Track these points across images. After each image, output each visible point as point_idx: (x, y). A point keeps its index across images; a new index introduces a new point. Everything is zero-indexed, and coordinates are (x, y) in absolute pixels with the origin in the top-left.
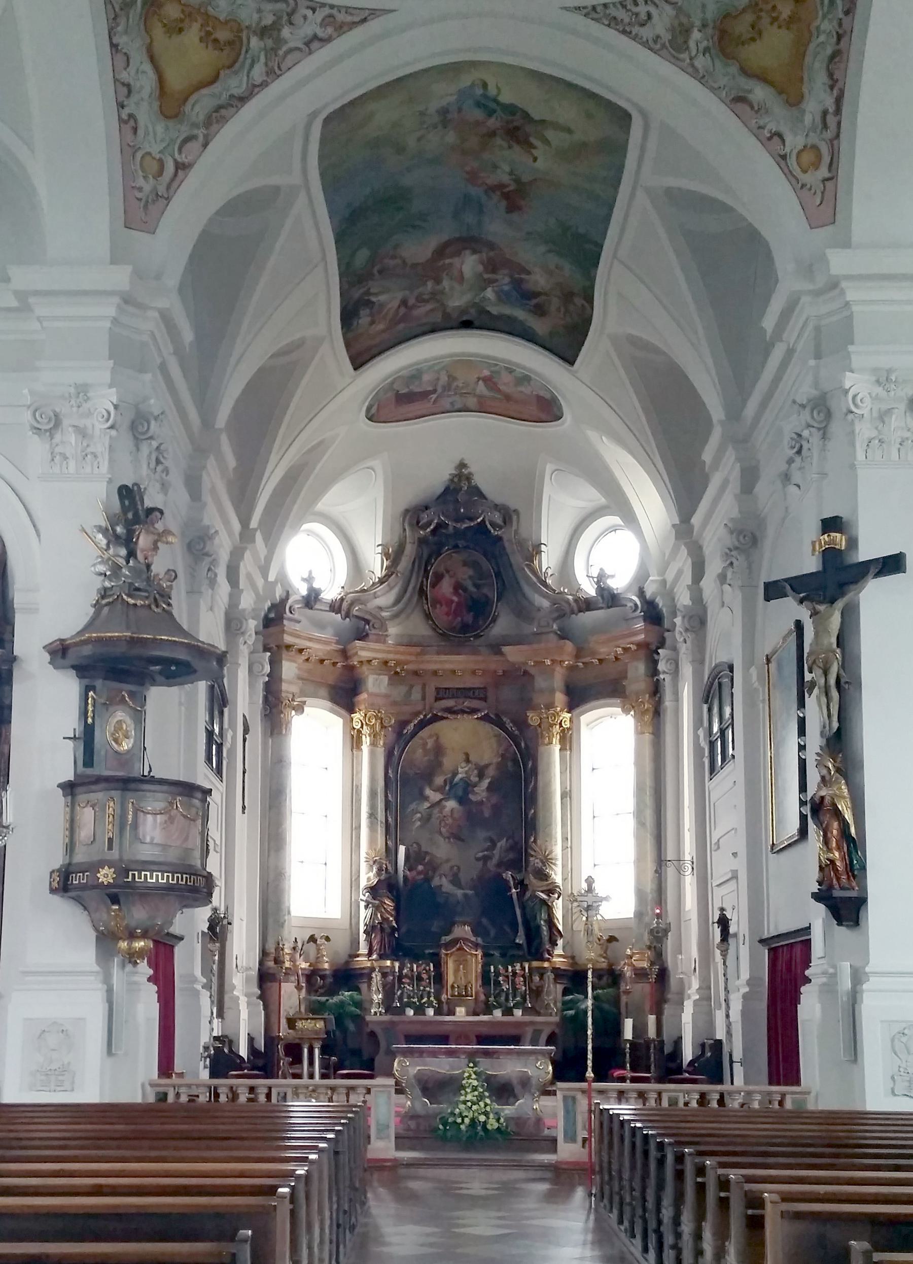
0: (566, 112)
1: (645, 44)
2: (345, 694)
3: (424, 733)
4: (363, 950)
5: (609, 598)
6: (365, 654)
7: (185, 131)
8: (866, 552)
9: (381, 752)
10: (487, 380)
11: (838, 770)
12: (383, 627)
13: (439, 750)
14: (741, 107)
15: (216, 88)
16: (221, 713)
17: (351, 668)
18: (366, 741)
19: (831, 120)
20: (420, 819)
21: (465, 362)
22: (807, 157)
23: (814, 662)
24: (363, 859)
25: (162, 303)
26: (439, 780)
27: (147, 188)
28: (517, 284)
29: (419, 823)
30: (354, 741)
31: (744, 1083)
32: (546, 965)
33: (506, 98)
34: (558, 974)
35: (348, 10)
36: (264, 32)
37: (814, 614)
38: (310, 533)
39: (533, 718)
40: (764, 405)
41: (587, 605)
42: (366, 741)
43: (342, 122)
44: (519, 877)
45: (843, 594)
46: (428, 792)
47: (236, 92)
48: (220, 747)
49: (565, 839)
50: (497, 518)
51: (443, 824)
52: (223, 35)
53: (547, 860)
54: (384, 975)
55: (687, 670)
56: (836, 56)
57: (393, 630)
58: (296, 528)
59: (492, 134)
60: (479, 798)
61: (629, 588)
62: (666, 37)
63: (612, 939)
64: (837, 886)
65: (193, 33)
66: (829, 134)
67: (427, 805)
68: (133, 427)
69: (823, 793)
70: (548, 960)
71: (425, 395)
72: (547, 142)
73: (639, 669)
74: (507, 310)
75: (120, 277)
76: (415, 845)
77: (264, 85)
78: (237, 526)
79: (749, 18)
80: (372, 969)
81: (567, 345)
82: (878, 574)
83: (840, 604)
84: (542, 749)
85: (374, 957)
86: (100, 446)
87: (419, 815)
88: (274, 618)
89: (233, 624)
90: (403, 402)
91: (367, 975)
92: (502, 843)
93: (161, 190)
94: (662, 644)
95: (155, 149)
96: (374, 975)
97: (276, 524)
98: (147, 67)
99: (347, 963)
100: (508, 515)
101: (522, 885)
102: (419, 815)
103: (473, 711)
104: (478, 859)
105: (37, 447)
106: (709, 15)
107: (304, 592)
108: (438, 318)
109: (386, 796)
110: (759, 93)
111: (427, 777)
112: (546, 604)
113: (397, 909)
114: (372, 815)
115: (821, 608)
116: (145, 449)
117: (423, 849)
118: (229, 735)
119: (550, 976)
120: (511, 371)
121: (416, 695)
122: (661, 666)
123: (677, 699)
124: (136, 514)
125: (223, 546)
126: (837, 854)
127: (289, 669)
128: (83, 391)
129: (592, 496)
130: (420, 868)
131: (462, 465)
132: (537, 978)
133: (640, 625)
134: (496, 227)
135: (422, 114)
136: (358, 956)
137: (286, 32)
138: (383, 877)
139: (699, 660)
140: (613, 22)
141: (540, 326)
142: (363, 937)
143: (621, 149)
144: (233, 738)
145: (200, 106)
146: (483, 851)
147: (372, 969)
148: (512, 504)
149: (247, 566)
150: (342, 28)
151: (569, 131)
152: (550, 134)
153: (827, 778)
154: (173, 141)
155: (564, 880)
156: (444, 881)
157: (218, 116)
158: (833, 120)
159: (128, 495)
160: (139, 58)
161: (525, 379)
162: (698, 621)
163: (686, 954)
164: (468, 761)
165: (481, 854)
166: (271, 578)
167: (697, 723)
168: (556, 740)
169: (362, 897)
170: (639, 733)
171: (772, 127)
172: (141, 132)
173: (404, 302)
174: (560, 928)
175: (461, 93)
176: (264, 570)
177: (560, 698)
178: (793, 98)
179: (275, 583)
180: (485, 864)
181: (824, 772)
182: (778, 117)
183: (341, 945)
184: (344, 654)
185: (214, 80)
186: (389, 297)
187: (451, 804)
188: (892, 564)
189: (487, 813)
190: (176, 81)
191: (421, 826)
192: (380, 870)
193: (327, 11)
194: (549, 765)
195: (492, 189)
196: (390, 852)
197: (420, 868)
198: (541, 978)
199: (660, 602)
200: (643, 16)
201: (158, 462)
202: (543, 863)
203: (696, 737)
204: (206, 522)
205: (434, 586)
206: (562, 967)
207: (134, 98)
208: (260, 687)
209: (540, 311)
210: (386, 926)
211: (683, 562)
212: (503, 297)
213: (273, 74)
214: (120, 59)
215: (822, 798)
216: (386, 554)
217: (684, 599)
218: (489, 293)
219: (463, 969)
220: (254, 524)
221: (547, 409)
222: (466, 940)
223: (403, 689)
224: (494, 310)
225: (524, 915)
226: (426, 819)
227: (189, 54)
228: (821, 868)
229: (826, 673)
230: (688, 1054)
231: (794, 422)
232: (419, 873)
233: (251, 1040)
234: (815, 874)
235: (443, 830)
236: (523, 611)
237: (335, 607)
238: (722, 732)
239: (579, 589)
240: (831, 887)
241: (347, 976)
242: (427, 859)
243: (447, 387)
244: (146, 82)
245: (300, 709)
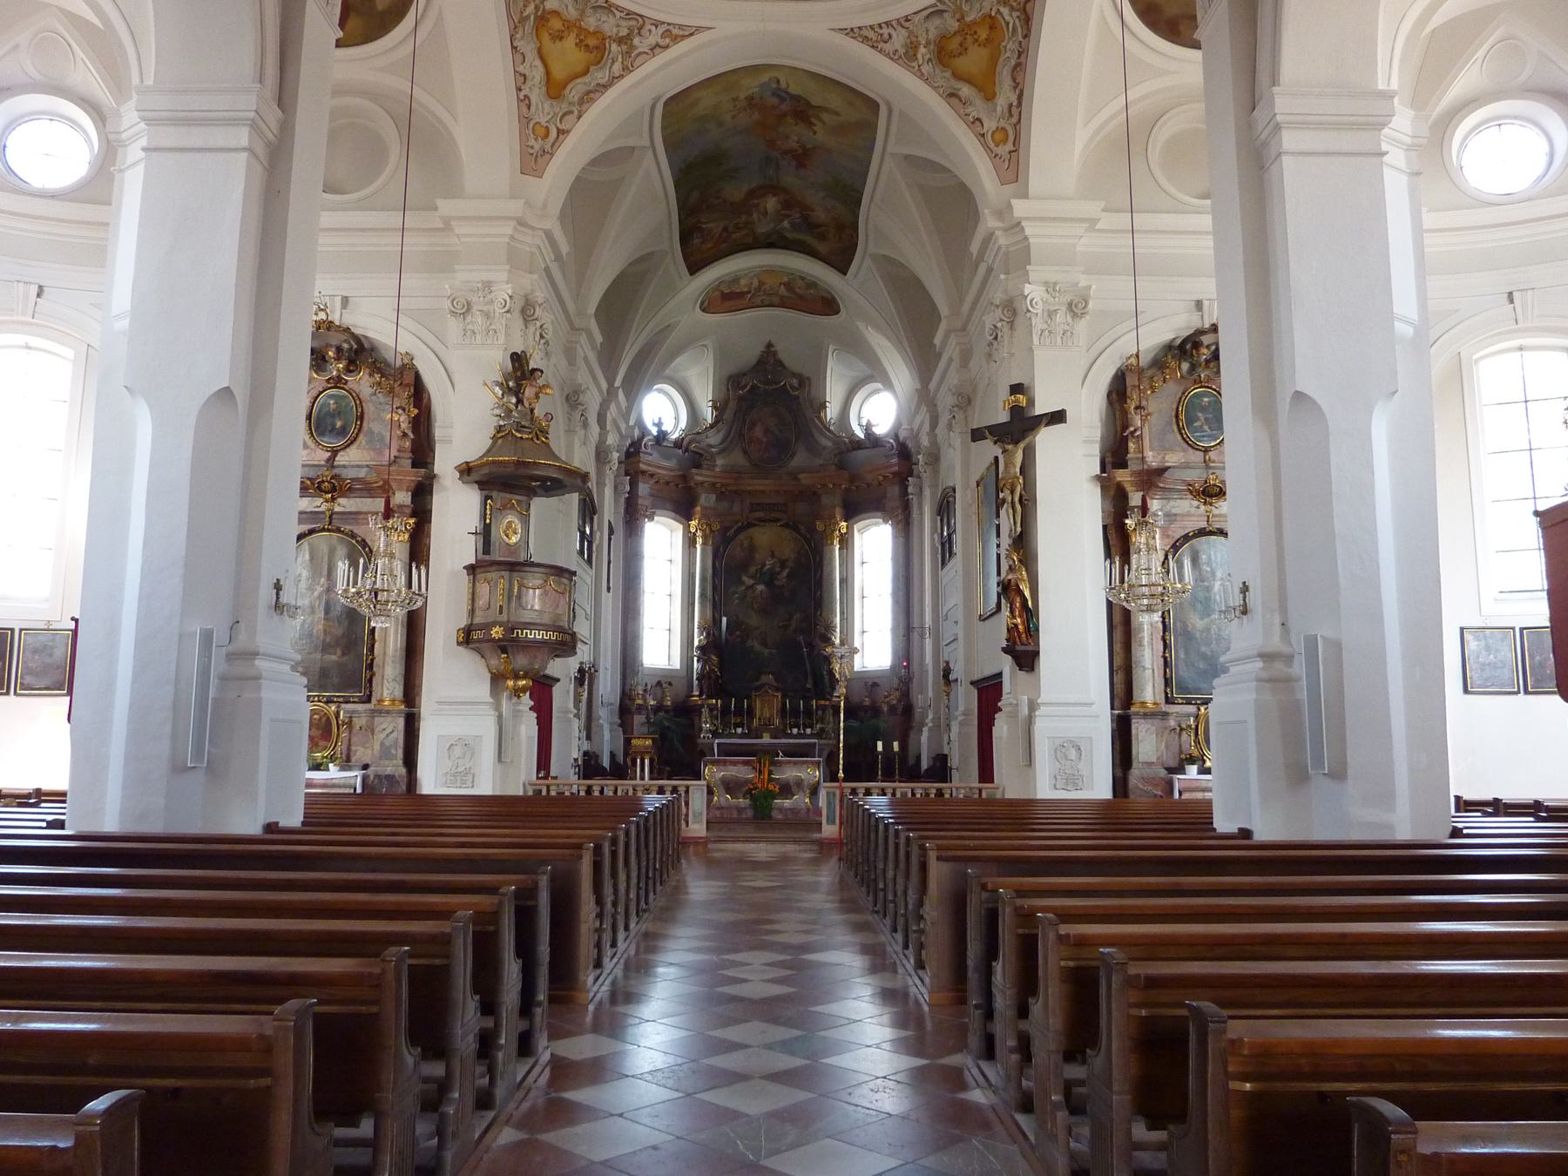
0: (834, 101)
1: (888, 55)
2: (683, 509)
3: (741, 536)
5: (872, 441)
6: (699, 478)
7: (565, 108)
9: (710, 549)
10: (788, 285)
12: (713, 457)
13: (752, 549)
14: (954, 101)
15: (586, 79)
16: (592, 520)
17: (690, 488)
18: (699, 541)
19: (1015, 111)
21: (771, 271)
22: (999, 136)
25: (547, 225)
26: (753, 569)
27: (537, 147)
28: (805, 218)
30: (690, 542)
31: (963, 781)
33: (793, 90)
35: (681, 27)
36: (620, 41)
38: (660, 391)
39: (820, 526)
40: (973, 308)
41: (857, 445)
42: (699, 541)
43: (677, 105)
46: (745, 579)
47: (602, 81)
48: (590, 544)
49: (842, 613)
50: (795, 382)
52: (592, 42)
53: (830, 628)
55: (927, 492)
56: (1018, 65)
57: (720, 462)
58: (649, 388)
59: (785, 115)
61: (887, 435)
62: (901, 51)
65: (570, 41)
66: (1014, 120)
68: (523, 311)
71: (741, 295)
72: (820, 120)
73: (894, 490)
74: (801, 237)
75: (516, 207)
77: (622, 76)
78: (604, 385)
79: (958, 39)
81: (841, 261)
84: (826, 549)
86: (499, 324)
88: (632, 452)
89: (601, 455)
90: (726, 299)
91: (697, 710)
92: (797, 616)
93: (548, 148)
94: (911, 474)
95: (543, 121)
97: (635, 385)
98: (538, 63)
100: (804, 381)
101: (811, 646)
103: (776, 520)
105: (453, 326)
106: (931, 36)
107: (654, 431)
108: (750, 240)
110: (965, 90)
111: (743, 567)
112: (830, 444)
114: (702, 595)
116: (532, 329)
118: (598, 535)
120: (803, 279)
121: (736, 508)
122: (910, 490)
123: (921, 514)
124: (523, 373)
125: (592, 400)
127: (644, 488)
128: (488, 285)
129: (861, 368)
131: (770, 345)
133: (895, 460)
134: (789, 179)
135: (734, 100)
137: (636, 41)
139: (934, 486)
140: (866, 39)
141: (822, 248)
143: (873, 127)
144: (601, 538)
145: (575, 91)
148: (806, 374)
149: (612, 412)
150: (676, 39)
151: (837, 114)
152: (825, 116)
154: (555, 115)
157: (587, 98)
158: (1017, 111)
159: (518, 359)
160: (532, 56)
161: (812, 285)
162: (935, 458)
163: (926, 693)
164: (773, 556)
166: (631, 423)
167: (933, 531)
168: (836, 542)
170: (895, 537)
171: (975, 114)
172: (533, 108)
173: (725, 229)
175: (762, 86)
176: (626, 415)
177: (838, 513)
178: (990, 97)
179: (633, 428)
182: (978, 108)
183: (680, 688)
184: (684, 478)
185: (586, 72)
186: (714, 225)
190: (559, 73)
193: (664, 27)
194: (832, 559)
195: (786, 152)
196: (716, 622)
199: (910, 444)
200: (886, 36)
201: (542, 337)
203: (933, 539)
204: (580, 380)
205: (750, 429)
207: (529, 84)
208: (622, 501)
209: (822, 237)
211: (923, 417)
212: (794, 226)
213: (627, 70)
214: (519, 58)
216: (714, 407)
217: (925, 442)
218: (786, 224)
219: (767, 707)
220: (617, 383)
221: (828, 306)
222: (770, 686)
223: (726, 504)
224: (789, 235)
226: (743, 598)
227: (567, 54)
230: (924, 765)
231: (989, 321)
233: (613, 755)
236: (814, 449)
237: (678, 444)
238: (949, 535)
239: (853, 434)
243: (759, 289)
244: (537, 73)
245: (651, 518)
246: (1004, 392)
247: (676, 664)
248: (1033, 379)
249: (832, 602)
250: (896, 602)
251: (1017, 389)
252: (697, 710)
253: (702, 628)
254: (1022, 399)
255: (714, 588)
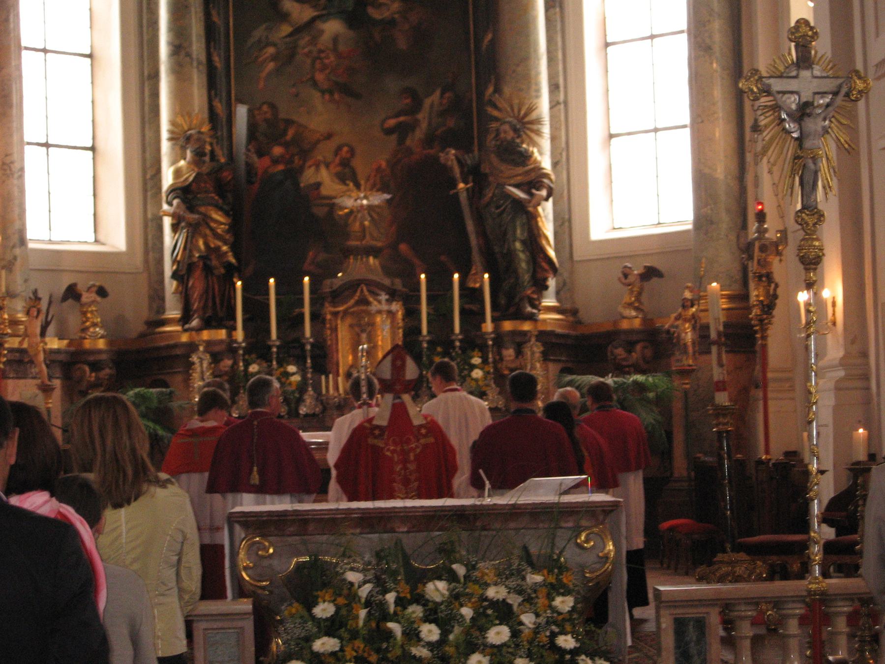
4: (173, 312)
20: (274, 58)
24: (165, 135)
29: (271, 65)
32: (527, 327)
34: (552, 344)
44: (469, 160)
49: (554, 87)
51: (318, 65)
54: (216, 358)
60: (385, 14)
63: (651, 273)
67: (286, 29)
70: (532, 318)
76: (265, 108)
80: (192, 347)
85: (195, 323)
87: (271, 50)
96: (195, 358)
99: (142, 336)
101: (477, 175)
102: (271, 50)
104: (389, 132)
109: (207, 15)
113: (234, 227)
114: (178, 48)
117: (282, 115)
119: (535, 349)
130: (277, 151)
132: (509, 353)
136: (164, 323)
138: (205, 169)
142: (170, 286)
146: (397, 115)
147: (192, 347)
155: (555, 164)
156: (324, 175)
165: (392, 122)
169: (165, 207)
174: (552, 253)
180: (401, 141)
187: (333, 27)
189: (402, 43)
191: (278, 71)
192: (199, 154)
196: (219, 121)
197: (277, 151)
198: (519, 352)
202: (516, 130)
206: (559, 331)
210: (214, 262)
225: (482, 233)
226: (287, 57)
232: (276, 161)
235: (320, 77)
241: (143, 360)
242: (290, 133)
247: (117, 239)
249: (526, 58)
250: (700, 46)
252: (176, 359)
253: (181, 139)
255: (210, 33)
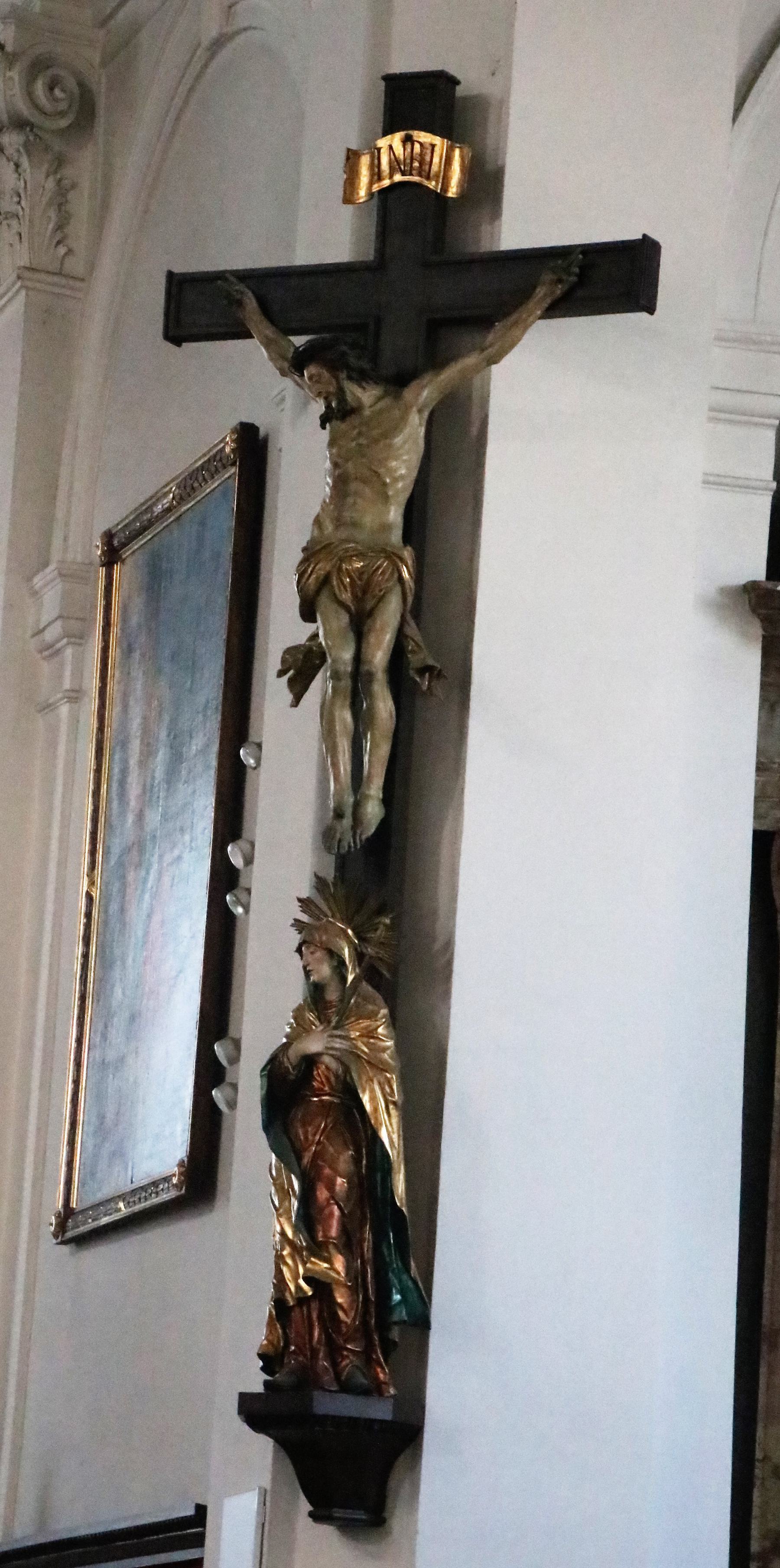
8: (520, 226)
11: (370, 973)
23: (325, 581)
37: (337, 413)
45: (435, 361)
64: (328, 1378)
69: (314, 1045)
82: (557, 309)
83: (425, 392)
115: (366, 396)
126: (339, 1263)
153: (332, 995)
181: (324, 971)
188: (613, 278)
215: (310, 1061)
228: (282, 1310)
229: (360, 625)
234: (254, 1328)
240: (307, 1380)
246: (337, 109)
248: (500, 66)
251: (419, 100)
254: (447, 166)
